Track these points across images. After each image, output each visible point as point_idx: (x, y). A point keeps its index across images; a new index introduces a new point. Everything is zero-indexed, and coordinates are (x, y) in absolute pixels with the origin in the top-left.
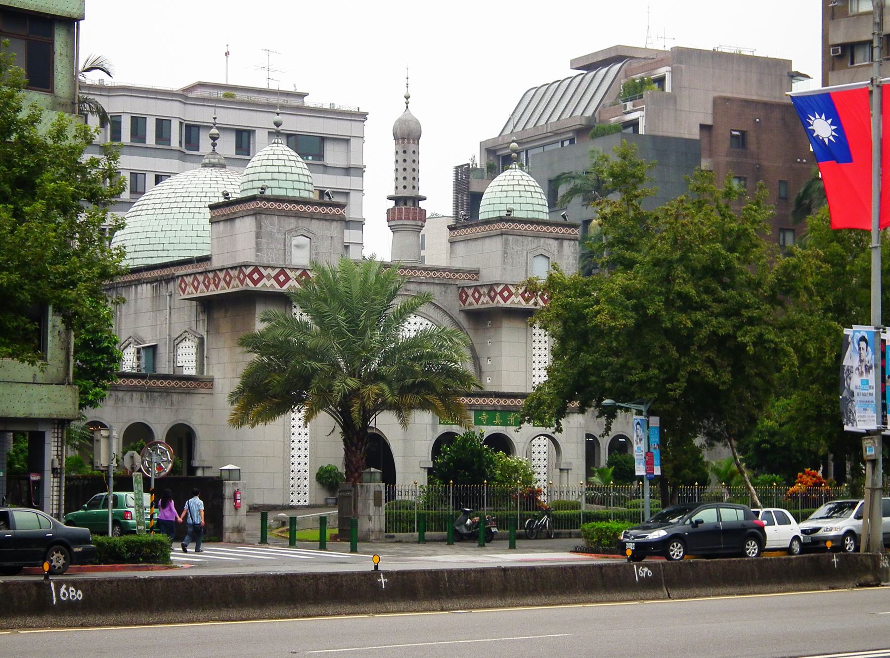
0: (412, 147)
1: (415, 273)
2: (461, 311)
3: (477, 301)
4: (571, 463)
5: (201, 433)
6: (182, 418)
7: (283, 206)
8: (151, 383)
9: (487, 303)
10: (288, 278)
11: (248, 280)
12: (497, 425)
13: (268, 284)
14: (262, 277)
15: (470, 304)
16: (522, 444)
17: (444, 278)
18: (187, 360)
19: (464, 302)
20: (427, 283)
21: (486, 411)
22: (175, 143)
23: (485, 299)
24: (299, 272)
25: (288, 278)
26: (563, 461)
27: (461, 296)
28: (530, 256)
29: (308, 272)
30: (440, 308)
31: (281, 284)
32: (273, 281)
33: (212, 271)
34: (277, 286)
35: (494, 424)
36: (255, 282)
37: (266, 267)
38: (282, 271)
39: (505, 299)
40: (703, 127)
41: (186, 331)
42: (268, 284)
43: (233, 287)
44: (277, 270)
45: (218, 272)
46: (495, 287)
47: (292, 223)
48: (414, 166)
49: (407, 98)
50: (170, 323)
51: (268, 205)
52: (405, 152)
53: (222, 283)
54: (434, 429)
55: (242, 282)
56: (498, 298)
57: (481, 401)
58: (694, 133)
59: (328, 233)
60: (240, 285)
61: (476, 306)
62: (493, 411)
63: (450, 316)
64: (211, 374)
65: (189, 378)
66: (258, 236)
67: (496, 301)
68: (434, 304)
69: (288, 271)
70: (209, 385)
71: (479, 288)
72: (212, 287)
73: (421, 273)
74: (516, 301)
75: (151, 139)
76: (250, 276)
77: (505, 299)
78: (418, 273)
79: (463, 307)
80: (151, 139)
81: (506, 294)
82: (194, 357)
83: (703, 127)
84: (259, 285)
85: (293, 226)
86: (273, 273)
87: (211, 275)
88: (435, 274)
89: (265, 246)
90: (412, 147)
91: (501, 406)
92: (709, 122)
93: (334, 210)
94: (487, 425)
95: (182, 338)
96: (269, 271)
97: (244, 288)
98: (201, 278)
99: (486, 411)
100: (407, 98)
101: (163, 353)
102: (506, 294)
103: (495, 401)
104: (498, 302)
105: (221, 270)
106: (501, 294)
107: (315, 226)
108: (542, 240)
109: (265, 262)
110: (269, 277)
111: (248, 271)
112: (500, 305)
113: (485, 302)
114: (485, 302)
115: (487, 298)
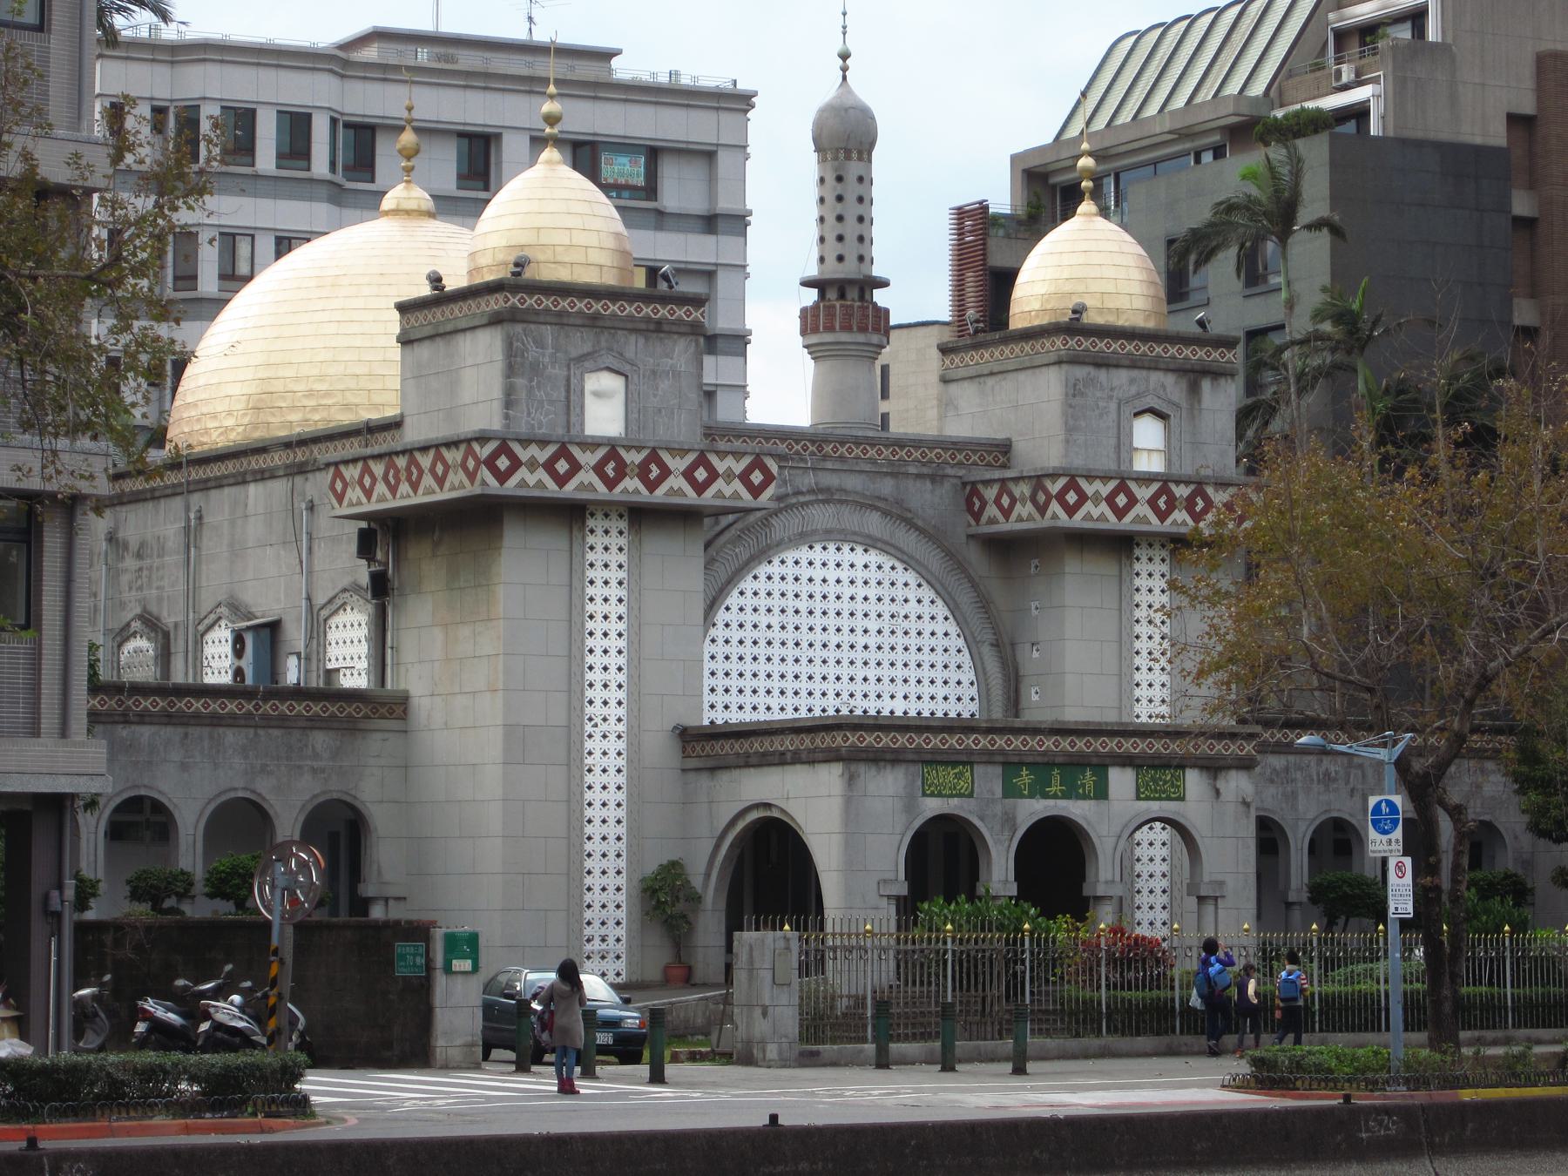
0: (854, 169)
2: (971, 537)
3: (1006, 513)
4: (1221, 883)
5: (380, 818)
6: (335, 788)
7: (564, 304)
8: (267, 707)
9: (1030, 518)
10: (575, 467)
11: (485, 473)
12: (1055, 797)
13: (532, 479)
14: (516, 464)
15: (992, 521)
16: (1111, 842)
17: (931, 462)
18: (348, 651)
19: (977, 516)
20: (894, 475)
21: (1028, 765)
22: (320, 164)
23: (1025, 510)
24: (601, 453)
25: (575, 467)
26: (1206, 878)
27: (969, 504)
28: (1128, 411)
29: (622, 452)
31: (561, 480)
32: (542, 474)
33: (403, 452)
34: (551, 484)
35: (1046, 796)
36: (502, 477)
37: (525, 442)
38: (563, 452)
39: (1071, 510)
40: (1513, 120)
41: (345, 590)
42: (531, 481)
43: (453, 488)
44: (551, 450)
45: (418, 455)
46: (1048, 483)
47: (580, 342)
48: (860, 210)
49: (845, 56)
50: (310, 573)
51: (531, 301)
52: (840, 179)
53: (428, 480)
54: (910, 807)
55: (472, 476)
56: (1055, 507)
57: (1017, 742)
58: (1496, 134)
60: (466, 482)
61: (1004, 526)
62: (1043, 767)
64: (402, 687)
65: (353, 696)
66: (511, 370)
67: (1049, 513)
69: (576, 451)
70: (399, 711)
71: (1011, 485)
72: (404, 488)
73: (880, 453)
74: (1096, 513)
75: (266, 158)
76: (490, 463)
77: (1071, 510)
79: (974, 530)
80: (266, 158)
81: (1071, 498)
82: (364, 649)
83: (1513, 120)
84: (512, 482)
85: (587, 348)
86: (543, 455)
87: (401, 462)
88: (909, 454)
89: (523, 395)
90: (854, 169)
91: (1065, 753)
92: (1527, 106)
93: (680, 312)
95: (336, 605)
96: (533, 450)
97: (477, 490)
98: (378, 469)
99: (1028, 765)
100: (845, 56)
101: (295, 635)
102: (1071, 498)
104: (1055, 517)
105: (424, 449)
106: (1061, 497)
107: (633, 346)
108: (1156, 377)
109: (522, 429)
110: (532, 465)
111: (485, 452)
112: (1059, 524)
113: (1025, 515)
114: (1025, 515)
115: (1029, 507)
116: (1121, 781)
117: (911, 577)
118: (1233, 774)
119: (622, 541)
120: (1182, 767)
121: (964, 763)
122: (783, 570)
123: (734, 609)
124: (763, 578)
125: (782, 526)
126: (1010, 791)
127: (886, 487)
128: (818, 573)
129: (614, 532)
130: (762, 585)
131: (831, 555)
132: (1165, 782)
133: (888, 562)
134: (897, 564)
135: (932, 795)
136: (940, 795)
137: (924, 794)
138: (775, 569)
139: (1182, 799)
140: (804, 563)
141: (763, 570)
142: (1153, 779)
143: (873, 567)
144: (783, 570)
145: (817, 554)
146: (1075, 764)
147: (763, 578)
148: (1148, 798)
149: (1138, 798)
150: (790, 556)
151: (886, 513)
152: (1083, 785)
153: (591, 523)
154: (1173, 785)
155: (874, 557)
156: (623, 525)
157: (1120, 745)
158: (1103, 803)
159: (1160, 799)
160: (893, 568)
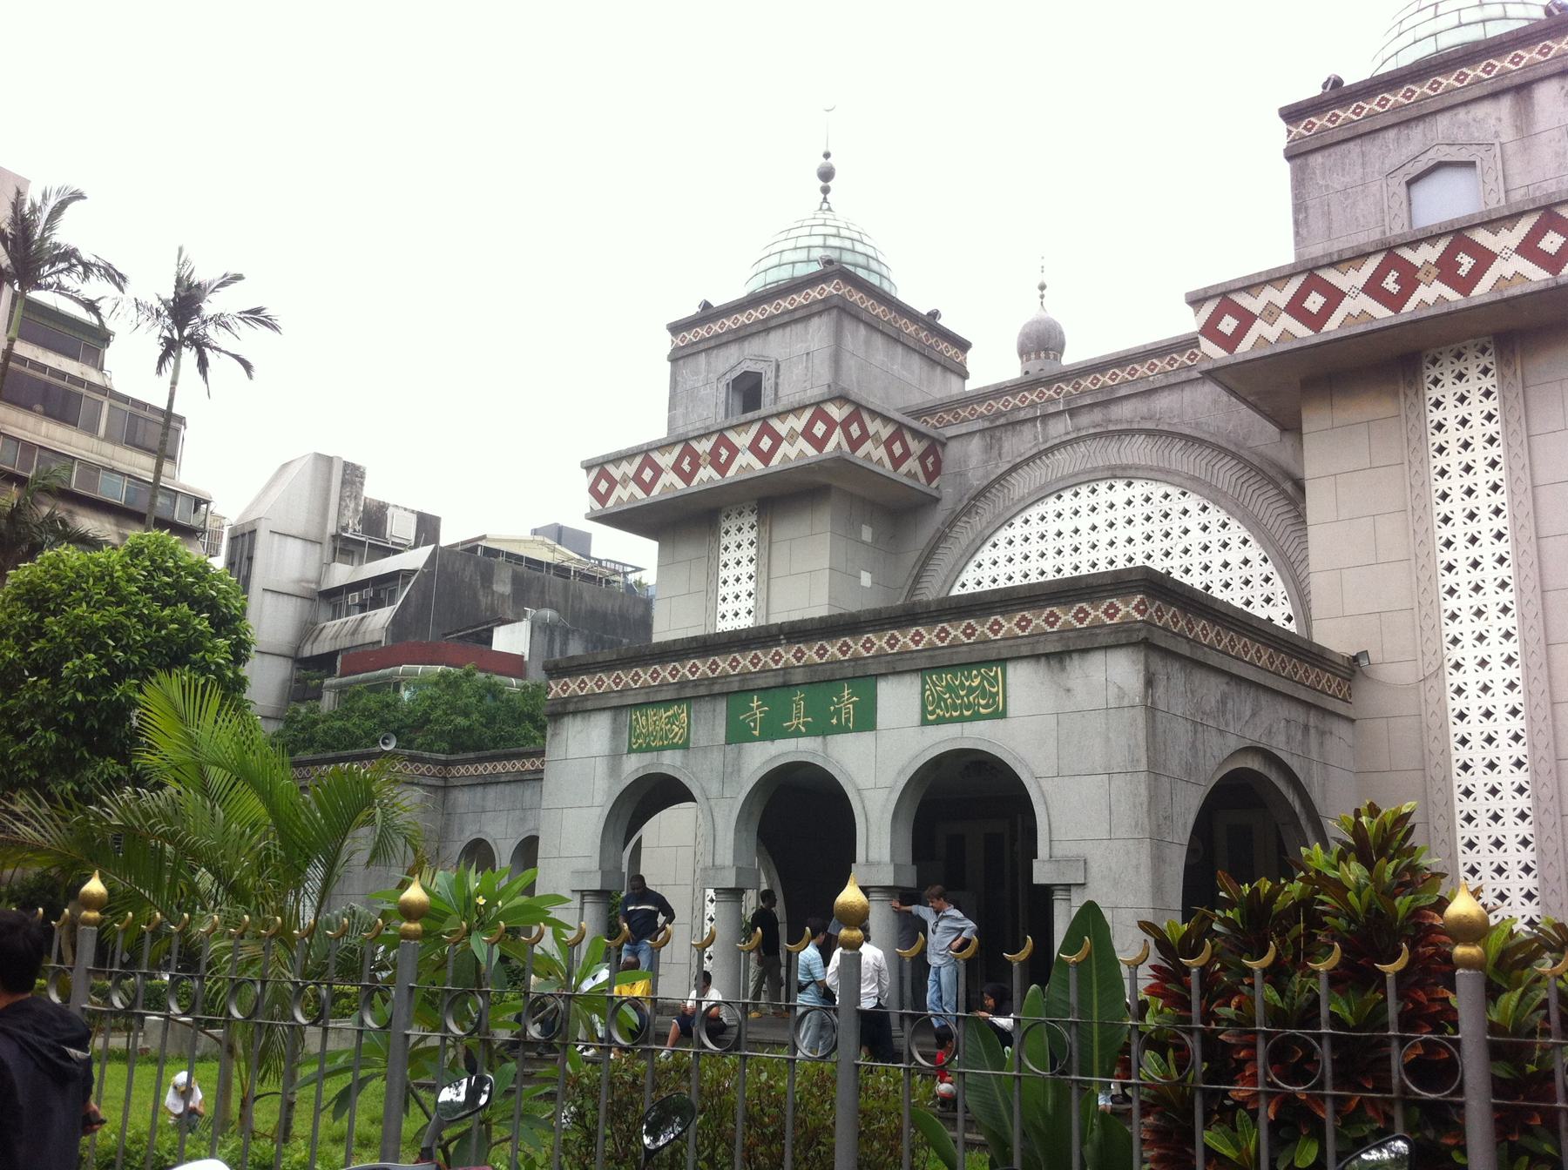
1: (1133, 372)
12: (797, 734)
20: (1170, 387)
30: (1201, 442)
59: (799, 348)
63: (1234, 456)
68: (1182, 436)
73: (1152, 367)
78: (1142, 370)
94: (762, 738)
103: (788, 655)
116: (898, 699)
117: (1192, 502)
118: (1097, 659)
119: (753, 535)
120: (1002, 661)
121: (677, 701)
122: (1026, 530)
123: (1247, 592)
124: (1002, 543)
125: (1022, 484)
126: (738, 735)
127: (1163, 402)
128: (1066, 525)
129: (746, 528)
130: (1002, 553)
131: (1085, 498)
132: (971, 690)
133: (1157, 490)
134: (1170, 490)
135: (640, 750)
136: (648, 749)
137: (631, 751)
138: (1017, 530)
139: (1001, 714)
140: (1050, 517)
141: (1002, 535)
142: (950, 688)
143: (1138, 501)
144: (1026, 530)
145: (1068, 501)
146: (824, 680)
147: (1002, 543)
148: (940, 721)
149: (925, 722)
150: (1034, 513)
151: (1149, 433)
152: (838, 712)
153: (725, 525)
154: (984, 694)
155: (1139, 489)
156: (753, 519)
157: (892, 642)
158: (867, 737)
159: (962, 719)
160: (1166, 496)
